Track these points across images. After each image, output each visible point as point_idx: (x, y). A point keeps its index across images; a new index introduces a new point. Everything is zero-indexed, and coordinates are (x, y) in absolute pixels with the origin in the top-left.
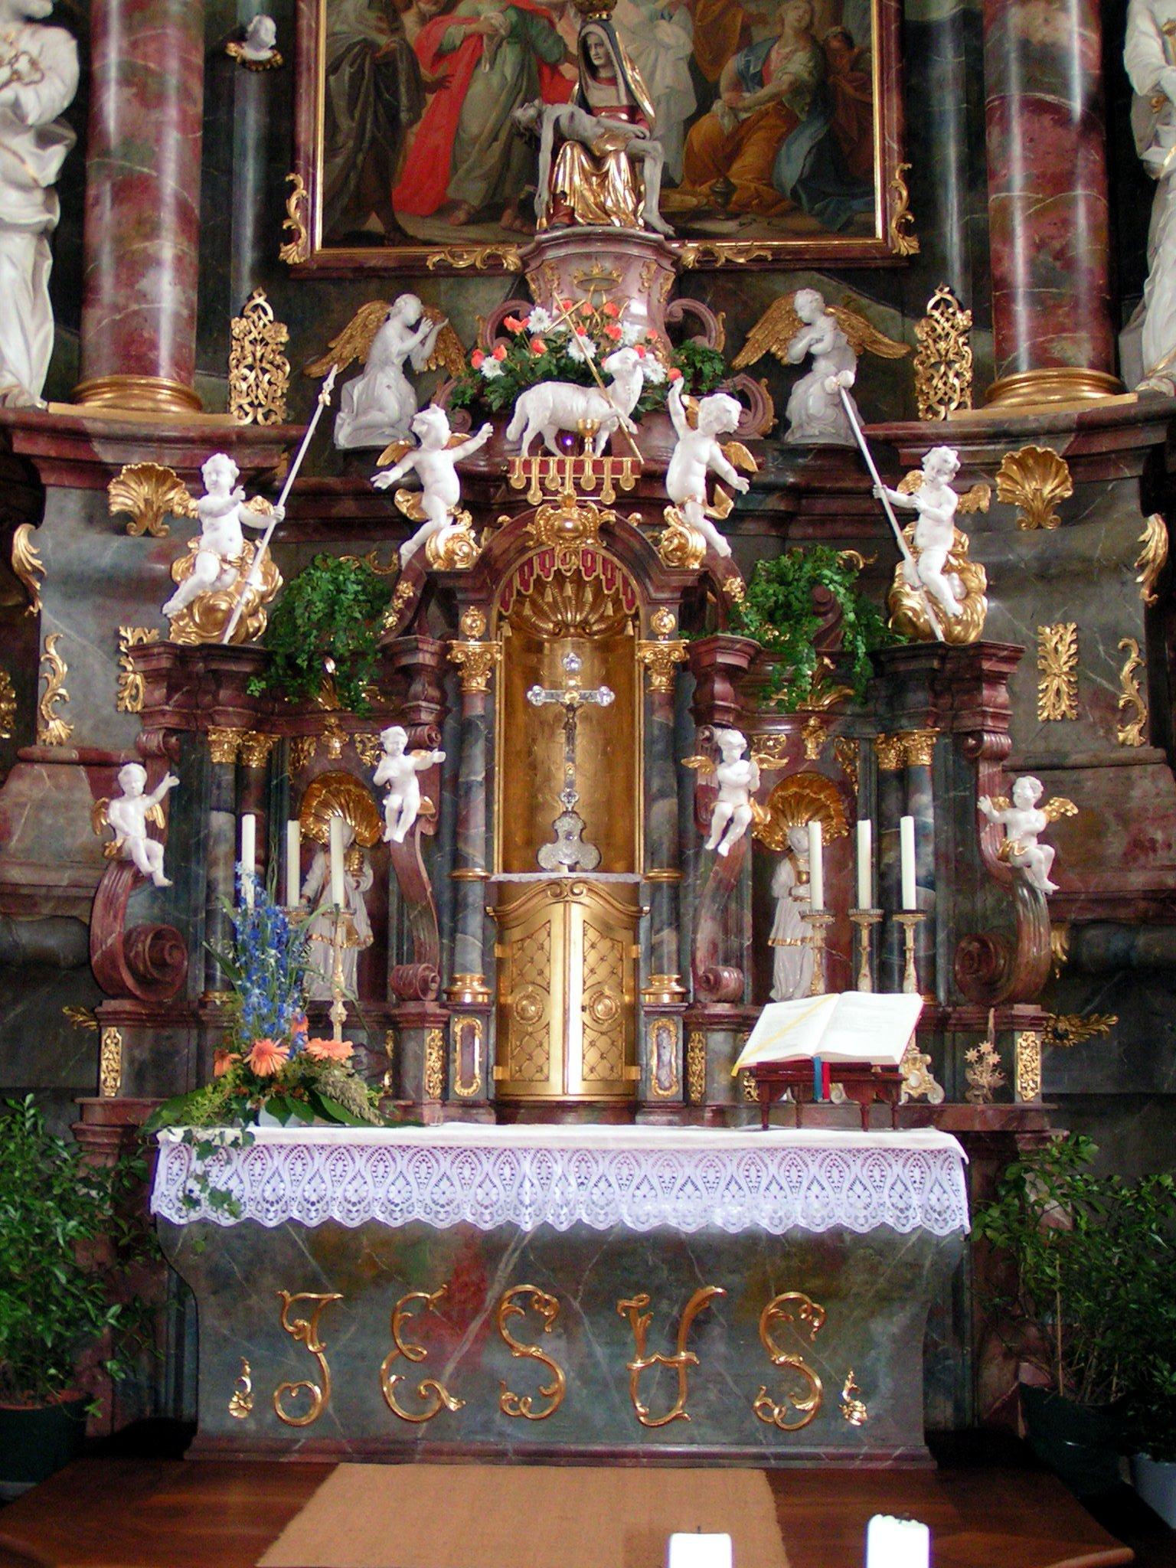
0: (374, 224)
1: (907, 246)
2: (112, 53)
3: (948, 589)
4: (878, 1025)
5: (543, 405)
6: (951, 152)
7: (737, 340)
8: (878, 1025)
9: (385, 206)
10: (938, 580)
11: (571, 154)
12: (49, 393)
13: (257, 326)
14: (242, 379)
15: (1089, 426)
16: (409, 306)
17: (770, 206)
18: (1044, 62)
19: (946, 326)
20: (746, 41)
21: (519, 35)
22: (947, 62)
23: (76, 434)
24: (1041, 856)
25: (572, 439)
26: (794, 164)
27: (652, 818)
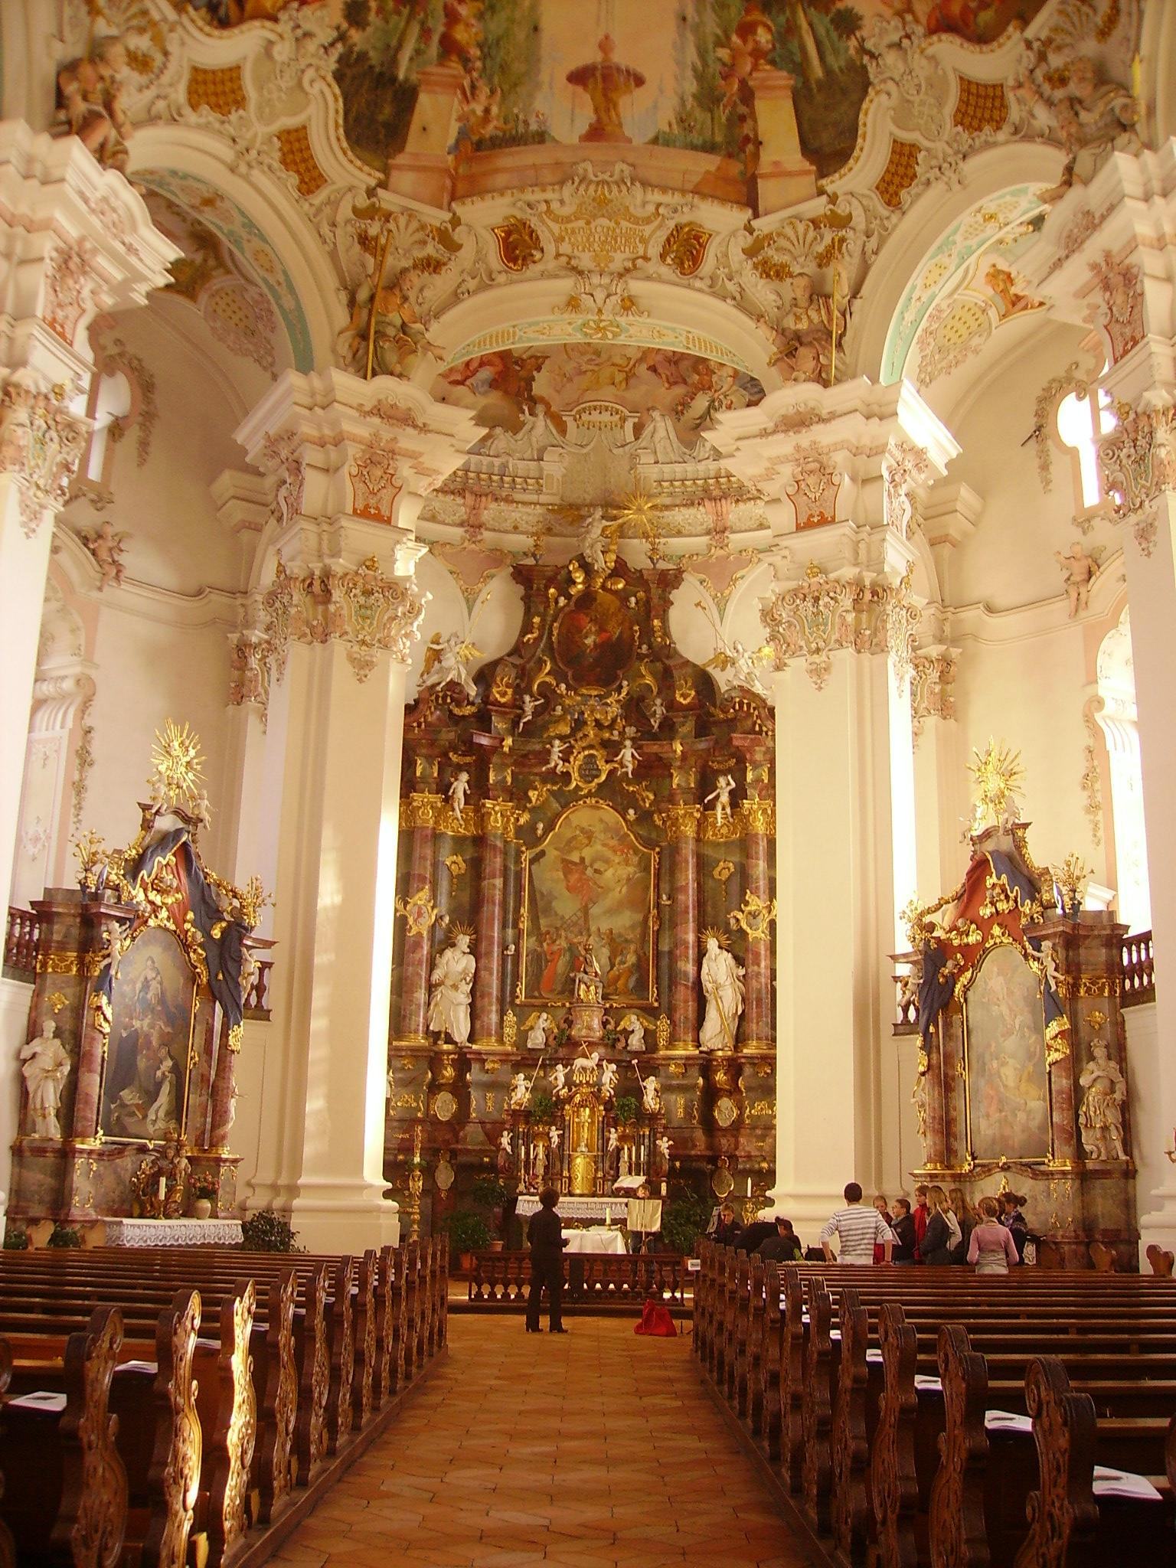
0: (536, 994)
1: (656, 1004)
2: (483, 961)
3: (652, 1103)
4: (635, 1181)
5: (580, 1062)
6: (665, 982)
7: (617, 1024)
8: (635, 1181)
9: (538, 990)
10: (650, 1101)
11: (583, 986)
12: (469, 1041)
13: (510, 1017)
14: (507, 1030)
15: (688, 1058)
16: (544, 1015)
17: (627, 992)
18: (686, 974)
19: (663, 1025)
20: (622, 953)
21: (570, 949)
22: (665, 962)
23: (479, 1053)
24: (666, 1152)
25: (584, 1069)
26: (632, 983)
27: (596, 1142)
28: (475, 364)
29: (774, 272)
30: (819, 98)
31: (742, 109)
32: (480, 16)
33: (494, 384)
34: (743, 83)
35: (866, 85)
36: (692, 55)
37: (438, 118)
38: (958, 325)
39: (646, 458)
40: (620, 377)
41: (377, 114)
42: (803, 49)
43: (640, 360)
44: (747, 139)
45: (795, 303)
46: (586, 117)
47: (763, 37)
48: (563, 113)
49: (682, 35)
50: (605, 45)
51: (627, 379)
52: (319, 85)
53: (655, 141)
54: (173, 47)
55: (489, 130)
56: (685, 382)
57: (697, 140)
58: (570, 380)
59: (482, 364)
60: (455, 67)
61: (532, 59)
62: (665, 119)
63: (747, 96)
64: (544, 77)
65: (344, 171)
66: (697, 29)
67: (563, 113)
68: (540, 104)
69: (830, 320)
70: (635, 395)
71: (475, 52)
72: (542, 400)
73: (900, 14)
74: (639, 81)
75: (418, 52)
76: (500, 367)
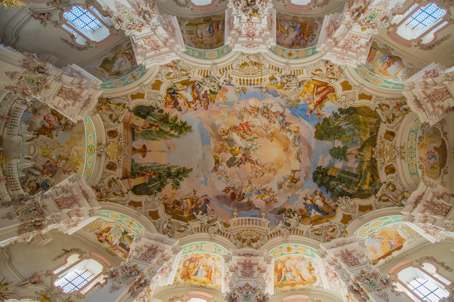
28: (50, 122)
29: (110, 184)
30: (145, 187)
31: (140, 175)
32: (156, 131)
33: (44, 126)
34: (145, 174)
35: (150, 195)
36: (149, 165)
37: (140, 122)
38: (95, 225)
39: (19, 161)
40: (46, 154)
41: (142, 112)
42: (153, 183)
43: (51, 159)
44: (135, 176)
45: (105, 189)
46: (137, 148)
47: (154, 177)
48: (138, 143)
49: (152, 163)
50: (150, 151)
51: (45, 156)
52: (151, 102)
53: (133, 160)
54: (169, 81)
55: (136, 131)
56: (44, 169)
57: (134, 167)
58: (44, 143)
59: (50, 124)
60: (148, 126)
61: (148, 139)
62: (137, 161)
63: (143, 175)
64: (145, 141)
65: (133, 104)
66: (154, 166)
67: (138, 143)
68: (140, 140)
69: (104, 197)
70: (40, 158)
71: (150, 130)
72: (38, 137)
73: (164, 198)
74: (144, 157)
75: (152, 120)
76: (49, 128)
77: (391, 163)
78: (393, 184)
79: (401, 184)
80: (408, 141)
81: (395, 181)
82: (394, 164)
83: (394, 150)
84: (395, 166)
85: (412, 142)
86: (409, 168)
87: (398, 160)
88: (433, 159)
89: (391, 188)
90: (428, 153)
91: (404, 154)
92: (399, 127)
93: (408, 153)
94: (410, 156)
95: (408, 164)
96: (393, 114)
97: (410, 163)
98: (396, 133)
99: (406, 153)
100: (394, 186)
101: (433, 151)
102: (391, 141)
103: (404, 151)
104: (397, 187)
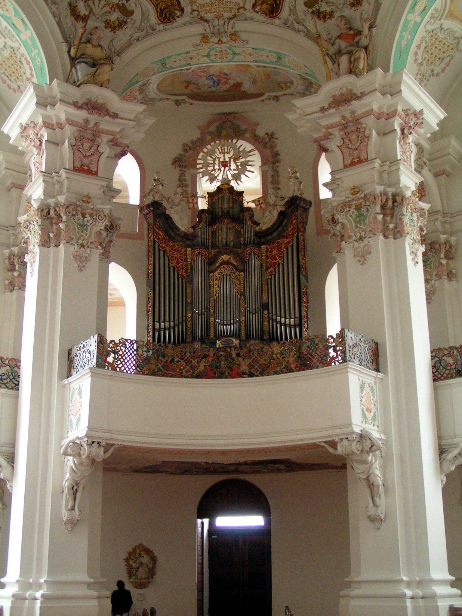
77: (188, 10)
78: (126, 22)
79: (129, 44)
80: (254, 49)
81: (137, 25)
82: (186, 18)
83: (227, 15)
84: (180, 21)
85: (250, 55)
86: (179, 55)
87: (198, 29)
88: (211, 83)
89: (115, 16)
90: (225, 74)
91: (216, 40)
92: (293, 29)
93: (218, 49)
94: (212, 53)
95: (188, 52)
96: (331, 15)
97: (191, 54)
98: (277, 21)
99: (218, 45)
100: (121, 24)
101: (232, 82)
102: (254, 6)
103: (224, 40)
104: (119, 32)
